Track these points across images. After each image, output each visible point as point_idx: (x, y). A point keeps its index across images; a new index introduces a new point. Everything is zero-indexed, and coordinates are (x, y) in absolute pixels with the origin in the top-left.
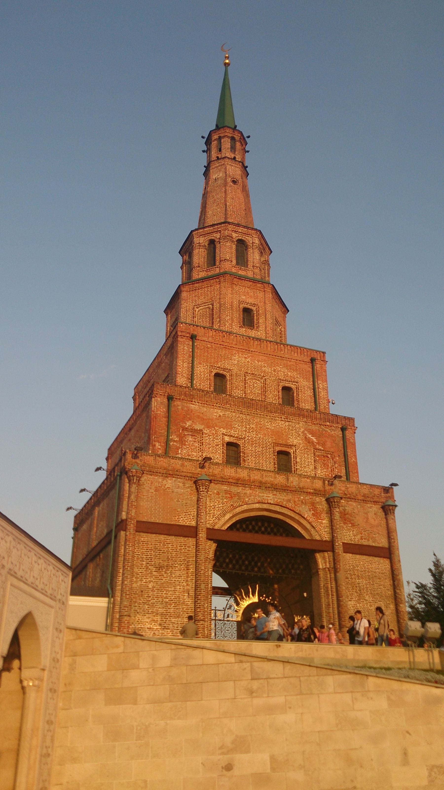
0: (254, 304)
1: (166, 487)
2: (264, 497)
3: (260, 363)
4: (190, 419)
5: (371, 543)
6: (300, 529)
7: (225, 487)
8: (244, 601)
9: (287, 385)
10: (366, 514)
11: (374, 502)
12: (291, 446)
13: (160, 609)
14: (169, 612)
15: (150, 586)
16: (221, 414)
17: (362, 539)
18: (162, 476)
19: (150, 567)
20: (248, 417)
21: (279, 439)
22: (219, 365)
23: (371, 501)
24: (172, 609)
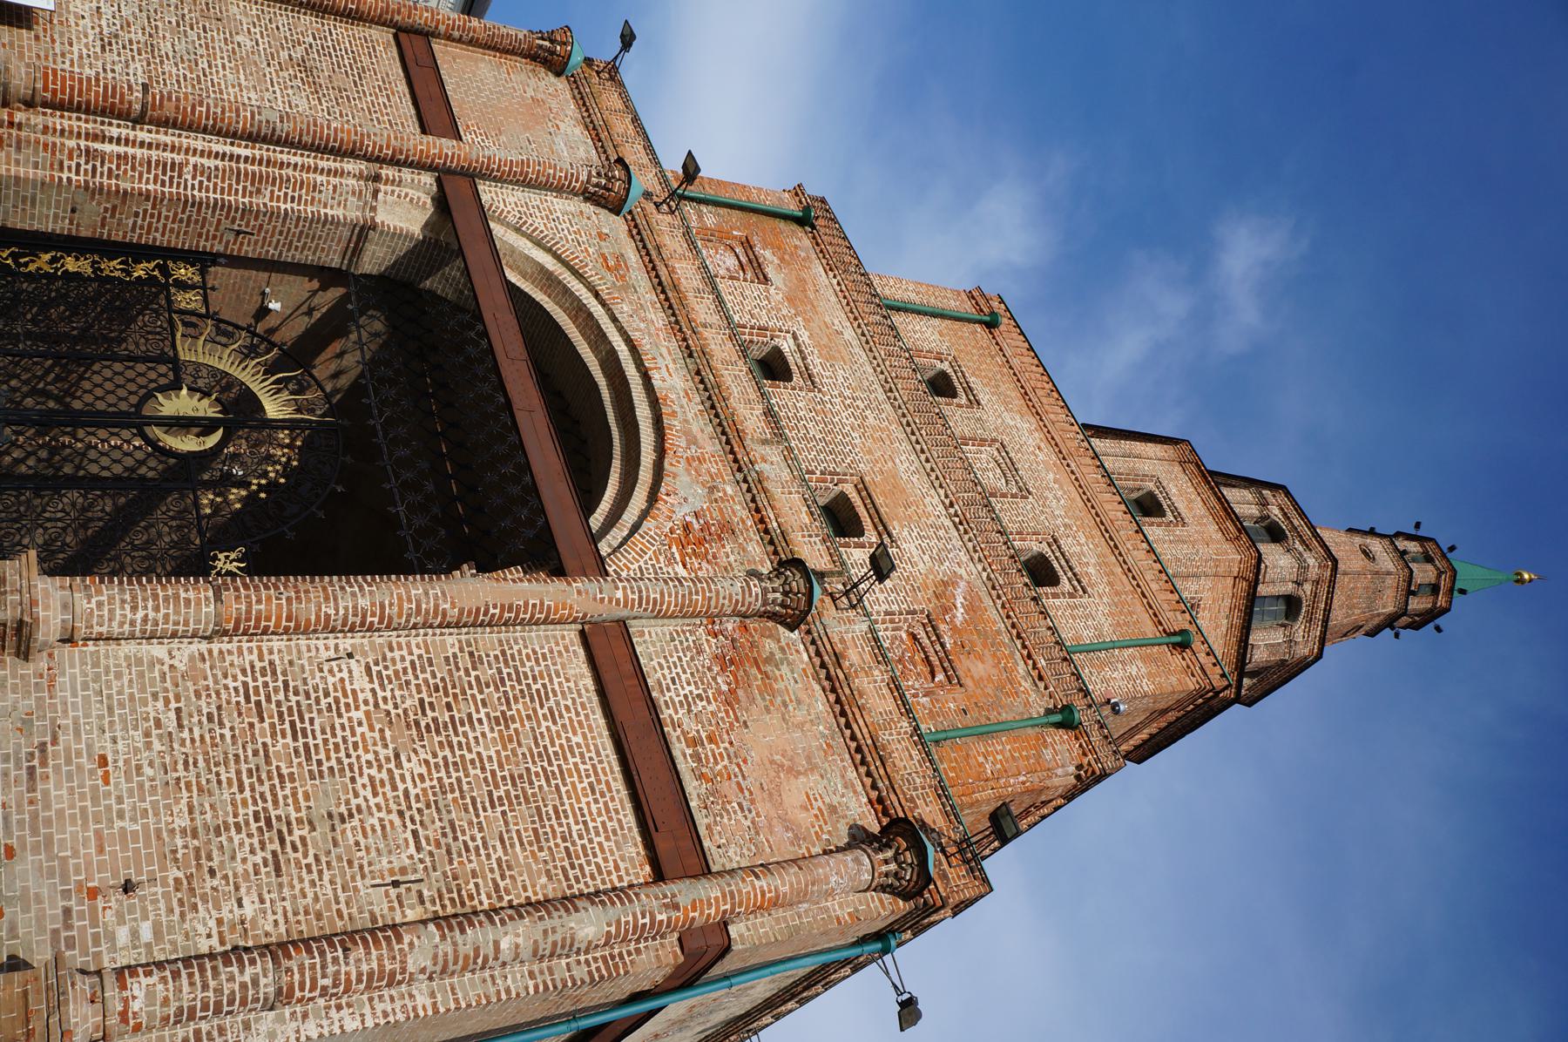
2: (660, 360)
4: (782, 259)
5: (692, 786)
6: (605, 506)
7: (633, 257)
8: (260, 377)
10: (813, 768)
11: (880, 800)
15: (239, 38)
16: (846, 336)
17: (694, 742)
20: (888, 407)
21: (884, 494)
22: (971, 379)
23: (874, 786)
24: (174, 70)
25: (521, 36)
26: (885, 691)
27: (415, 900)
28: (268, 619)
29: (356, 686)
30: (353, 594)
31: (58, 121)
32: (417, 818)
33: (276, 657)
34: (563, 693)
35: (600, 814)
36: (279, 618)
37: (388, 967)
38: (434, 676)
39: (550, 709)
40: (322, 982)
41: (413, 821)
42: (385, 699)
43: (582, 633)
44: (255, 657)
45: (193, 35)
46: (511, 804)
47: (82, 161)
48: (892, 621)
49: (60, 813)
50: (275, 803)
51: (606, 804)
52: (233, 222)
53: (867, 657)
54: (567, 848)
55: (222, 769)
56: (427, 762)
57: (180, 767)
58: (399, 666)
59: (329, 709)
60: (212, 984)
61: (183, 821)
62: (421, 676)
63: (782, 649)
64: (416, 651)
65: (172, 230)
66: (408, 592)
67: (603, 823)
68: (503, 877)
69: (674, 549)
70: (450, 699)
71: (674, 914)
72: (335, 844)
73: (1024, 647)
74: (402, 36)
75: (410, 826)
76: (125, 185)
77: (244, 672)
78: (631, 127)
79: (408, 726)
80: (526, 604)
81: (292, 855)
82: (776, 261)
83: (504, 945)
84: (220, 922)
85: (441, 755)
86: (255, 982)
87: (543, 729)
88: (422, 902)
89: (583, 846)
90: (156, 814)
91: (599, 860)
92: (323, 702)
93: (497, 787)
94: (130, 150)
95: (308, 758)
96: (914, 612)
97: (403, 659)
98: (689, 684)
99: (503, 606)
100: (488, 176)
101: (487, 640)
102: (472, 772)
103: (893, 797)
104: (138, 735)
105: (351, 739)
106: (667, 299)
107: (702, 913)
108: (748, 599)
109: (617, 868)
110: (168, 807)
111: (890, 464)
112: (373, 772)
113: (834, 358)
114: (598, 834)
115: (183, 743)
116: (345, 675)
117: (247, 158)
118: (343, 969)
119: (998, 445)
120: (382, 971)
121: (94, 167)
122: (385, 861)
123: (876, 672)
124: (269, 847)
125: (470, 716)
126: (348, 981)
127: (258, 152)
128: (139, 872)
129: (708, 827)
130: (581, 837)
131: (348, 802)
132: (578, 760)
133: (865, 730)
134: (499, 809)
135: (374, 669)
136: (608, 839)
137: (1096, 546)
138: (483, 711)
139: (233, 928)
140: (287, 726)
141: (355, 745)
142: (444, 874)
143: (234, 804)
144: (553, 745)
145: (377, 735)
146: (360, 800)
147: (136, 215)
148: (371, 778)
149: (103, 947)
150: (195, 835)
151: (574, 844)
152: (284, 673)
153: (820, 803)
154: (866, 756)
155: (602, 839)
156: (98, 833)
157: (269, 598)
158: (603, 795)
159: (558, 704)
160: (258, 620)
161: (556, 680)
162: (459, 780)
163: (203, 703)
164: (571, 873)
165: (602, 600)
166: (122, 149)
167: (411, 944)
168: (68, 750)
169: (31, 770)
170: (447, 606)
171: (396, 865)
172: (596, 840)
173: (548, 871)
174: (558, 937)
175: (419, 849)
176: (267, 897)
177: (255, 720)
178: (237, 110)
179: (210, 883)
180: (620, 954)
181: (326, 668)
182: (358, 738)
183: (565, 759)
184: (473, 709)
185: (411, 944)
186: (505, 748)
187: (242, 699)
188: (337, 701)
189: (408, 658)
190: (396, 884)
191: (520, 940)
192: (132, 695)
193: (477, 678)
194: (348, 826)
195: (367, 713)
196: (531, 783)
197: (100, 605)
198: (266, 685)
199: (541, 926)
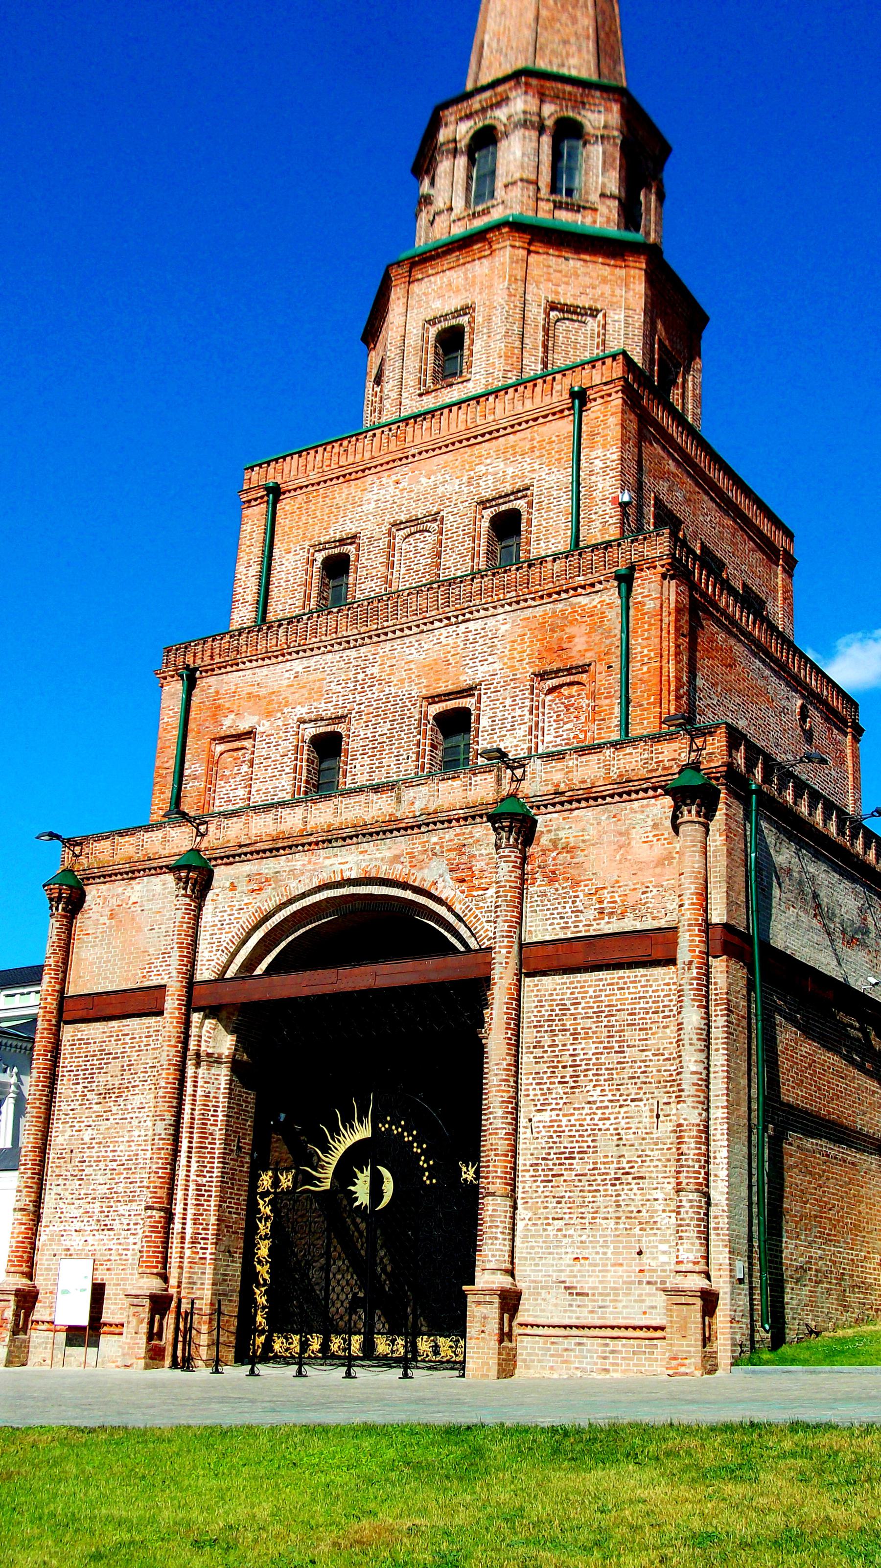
0: (462, 309)
1: (131, 902)
3: (433, 478)
8: (341, 1139)
9: (503, 508)
10: (626, 833)
12: (467, 692)
13: (100, 1187)
14: (116, 1193)
15: (87, 1139)
18: (123, 879)
19: (90, 1096)
20: (363, 649)
23: (645, 790)
24: (122, 1185)
25: (57, 925)
26: (584, 759)
27: (667, 1107)
28: (506, 1167)
29: (548, 1119)
30: (495, 1118)
31: (174, 1261)
32: (625, 1097)
33: (528, 1163)
34: (563, 994)
35: (636, 987)
36: (506, 1161)
37: (695, 1133)
38: (546, 1072)
39: (572, 1004)
40: (696, 1168)
41: (625, 1100)
42: (557, 1104)
43: (528, 975)
44: (527, 1174)
45: (88, 1171)
46: (623, 1041)
47: (199, 1246)
48: (537, 708)
49: (601, 1282)
50: (607, 1174)
51: (631, 982)
52: (232, 1150)
53: (560, 765)
54: (653, 1013)
55: (587, 1200)
56: (595, 1086)
57: (583, 1221)
58: (539, 1092)
59: (560, 1137)
60: (687, 1222)
61: (611, 1223)
62: (545, 1080)
63: (549, 831)
64: (531, 1081)
65: (238, 1190)
66: (495, 1086)
67: (642, 986)
68: (663, 1055)
69: (475, 893)
70: (560, 1065)
71: (694, 965)
72: (632, 1145)
73: (566, 591)
74: (65, 1017)
75: (628, 1102)
76: (213, 1220)
77: (535, 1181)
78: (127, 838)
79: (573, 1093)
80: (506, 1013)
81: (635, 1170)
82: (232, 716)
83: (694, 1068)
84: (664, 1211)
85: (591, 1077)
86: (691, 1201)
87: (583, 1011)
88: (669, 1103)
89: (654, 1002)
90: (606, 1236)
91: (662, 994)
92: (555, 1139)
93: (612, 1047)
94: (189, 1216)
95: (585, 1152)
96: (532, 687)
97: (534, 1089)
98: (565, 908)
99: (507, 1028)
100: (191, 973)
101: (528, 1036)
102: (603, 1061)
103: (654, 780)
104: (565, 1240)
105: (578, 1128)
106: (284, 848)
107: (697, 946)
108: (513, 859)
109: (668, 984)
110: (603, 1230)
111: (412, 666)
112: (597, 1117)
113: (320, 689)
114: (647, 992)
115: (571, 1218)
116: (541, 1125)
117: (190, 1142)
118: (691, 1156)
119: (394, 530)
120: (697, 1137)
121: (203, 1239)
122: (644, 1120)
123: (570, 763)
124: (630, 1180)
125: (571, 1055)
126: (698, 1154)
127: (184, 1135)
128: (635, 1247)
129: (654, 919)
130: (647, 1003)
131: (612, 1135)
132: (603, 994)
133: (608, 787)
134: (626, 1049)
135: (539, 1107)
136: (651, 986)
137: (489, 456)
138: (568, 1047)
139: (668, 1205)
140: (567, 1162)
141: (581, 1125)
142: (657, 1087)
143: (606, 1196)
144: (592, 1008)
145: (577, 1112)
146: (612, 1127)
147: (230, 1212)
148: (600, 1119)
149: (668, 1268)
150: (619, 1218)
151: (651, 1008)
152: (538, 1159)
153: (651, 835)
154: (625, 790)
155: (650, 990)
156: (614, 1265)
157: (494, 1166)
158: (625, 983)
159: (569, 999)
160: (506, 1173)
161: (555, 997)
162: (607, 1069)
163: (550, 1205)
164: (667, 1013)
165: (507, 963)
166: (189, 1222)
167: (685, 1119)
168: (570, 1276)
169: (577, 1294)
170: (505, 1063)
171: (648, 1114)
172: (650, 993)
173: (664, 1027)
174: (695, 1037)
175: (641, 1100)
176: (655, 1186)
177: (562, 1178)
178: (159, 1149)
179: (644, 1213)
180: (716, 994)
181: (536, 1135)
182: (578, 1123)
183: (601, 1001)
184: (567, 1053)
185: (685, 1119)
186: (591, 1038)
187: (550, 1184)
188: (555, 1132)
189: (534, 1086)
190: (658, 1116)
191: (693, 1059)
192: (544, 1242)
193: (549, 1046)
194: (624, 1137)
195: (564, 1115)
196: (613, 1026)
197: (493, 1256)
198: (543, 1170)
199: (687, 1046)
